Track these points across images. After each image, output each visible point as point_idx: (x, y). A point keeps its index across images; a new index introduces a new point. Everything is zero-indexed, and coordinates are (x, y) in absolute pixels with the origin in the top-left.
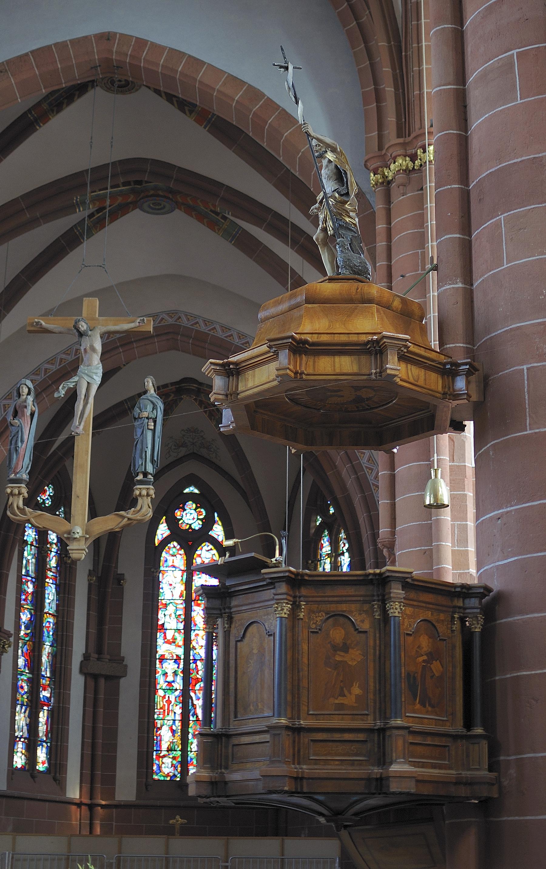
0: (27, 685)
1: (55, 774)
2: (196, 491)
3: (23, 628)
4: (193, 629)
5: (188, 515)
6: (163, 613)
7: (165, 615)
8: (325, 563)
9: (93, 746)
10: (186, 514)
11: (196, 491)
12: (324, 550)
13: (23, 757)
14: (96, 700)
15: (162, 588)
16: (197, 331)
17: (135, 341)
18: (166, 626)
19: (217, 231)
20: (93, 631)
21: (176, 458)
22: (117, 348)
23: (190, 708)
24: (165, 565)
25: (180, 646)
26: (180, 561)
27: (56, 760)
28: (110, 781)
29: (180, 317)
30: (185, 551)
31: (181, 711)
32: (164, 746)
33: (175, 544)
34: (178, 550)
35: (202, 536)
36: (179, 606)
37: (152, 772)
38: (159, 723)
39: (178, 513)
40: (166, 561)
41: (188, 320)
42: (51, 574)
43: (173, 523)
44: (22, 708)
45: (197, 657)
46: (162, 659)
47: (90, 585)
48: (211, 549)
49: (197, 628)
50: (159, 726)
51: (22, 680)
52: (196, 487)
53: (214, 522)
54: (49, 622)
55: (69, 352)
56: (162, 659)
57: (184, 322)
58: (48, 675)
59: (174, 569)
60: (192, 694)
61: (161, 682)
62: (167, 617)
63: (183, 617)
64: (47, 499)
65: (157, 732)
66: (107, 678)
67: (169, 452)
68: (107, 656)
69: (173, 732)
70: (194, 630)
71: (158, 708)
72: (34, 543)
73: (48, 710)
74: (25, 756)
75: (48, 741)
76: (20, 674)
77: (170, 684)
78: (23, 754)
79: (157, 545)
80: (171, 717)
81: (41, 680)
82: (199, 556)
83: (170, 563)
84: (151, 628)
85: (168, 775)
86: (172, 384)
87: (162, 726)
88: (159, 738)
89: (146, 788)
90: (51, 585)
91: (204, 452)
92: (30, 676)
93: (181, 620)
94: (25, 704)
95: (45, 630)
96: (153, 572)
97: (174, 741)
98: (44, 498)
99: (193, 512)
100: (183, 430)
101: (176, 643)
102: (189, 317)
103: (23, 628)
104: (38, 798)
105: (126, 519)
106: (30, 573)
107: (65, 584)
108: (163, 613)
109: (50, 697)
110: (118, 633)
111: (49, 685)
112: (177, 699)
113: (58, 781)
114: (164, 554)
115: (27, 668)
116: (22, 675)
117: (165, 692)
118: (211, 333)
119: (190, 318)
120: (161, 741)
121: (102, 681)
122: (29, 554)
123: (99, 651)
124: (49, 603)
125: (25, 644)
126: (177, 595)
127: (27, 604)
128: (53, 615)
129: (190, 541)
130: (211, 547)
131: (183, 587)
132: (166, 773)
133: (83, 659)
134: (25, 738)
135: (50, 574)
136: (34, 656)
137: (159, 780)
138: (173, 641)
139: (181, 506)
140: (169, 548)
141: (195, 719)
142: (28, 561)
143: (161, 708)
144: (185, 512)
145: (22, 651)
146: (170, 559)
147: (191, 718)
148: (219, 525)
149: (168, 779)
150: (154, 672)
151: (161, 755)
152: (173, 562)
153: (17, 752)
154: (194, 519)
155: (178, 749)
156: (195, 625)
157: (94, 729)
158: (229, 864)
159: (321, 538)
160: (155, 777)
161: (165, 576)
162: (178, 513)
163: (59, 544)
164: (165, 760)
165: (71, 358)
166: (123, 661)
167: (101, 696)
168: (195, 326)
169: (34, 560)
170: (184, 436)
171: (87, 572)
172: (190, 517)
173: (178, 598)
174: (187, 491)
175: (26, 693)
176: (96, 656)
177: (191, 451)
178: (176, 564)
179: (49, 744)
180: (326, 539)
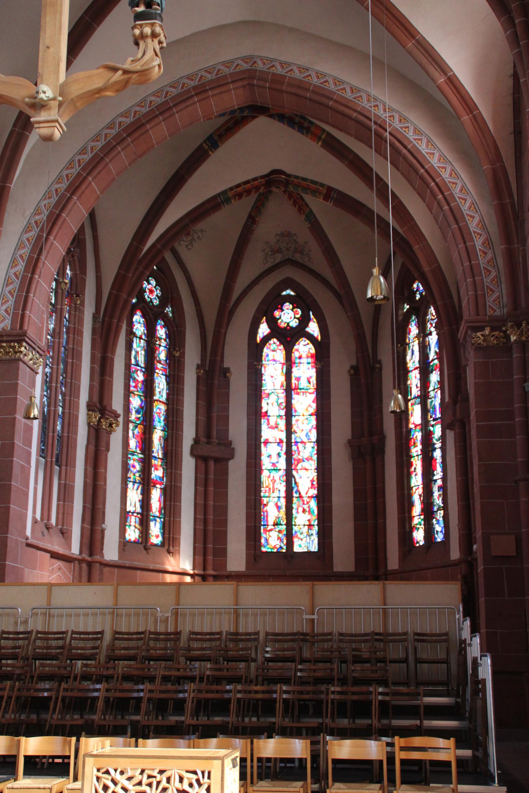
0: (139, 465)
1: (169, 546)
2: (292, 293)
3: (134, 412)
4: (294, 414)
5: (286, 314)
6: (266, 401)
7: (268, 404)
8: (413, 346)
9: (205, 521)
10: (284, 314)
11: (292, 293)
12: (412, 334)
13: (137, 531)
14: (206, 480)
15: (265, 380)
16: (273, 74)
18: (269, 414)
20: (202, 418)
21: (273, 264)
23: (293, 485)
24: (266, 360)
25: (282, 431)
26: (280, 355)
27: (169, 534)
28: (221, 553)
29: (255, 62)
30: (284, 346)
31: (285, 489)
32: (271, 521)
33: (275, 340)
34: (278, 346)
35: (300, 332)
36: (279, 395)
37: (260, 545)
38: (265, 500)
39: (277, 314)
40: (267, 356)
41: (264, 64)
42: (161, 366)
43: (273, 323)
44: (134, 485)
45: (299, 440)
46: (266, 442)
47: (198, 378)
48: (308, 344)
49: (297, 414)
50: (265, 502)
51: (134, 460)
52: (292, 290)
53: (309, 320)
54: (160, 409)
55: (143, 104)
56: (266, 442)
57: (260, 66)
58: (160, 456)
59: (275, 362)
60: (294, 473)
61: (266, 463)
62: (270, 405)
63: (284, 405)
64: (155, 299)
65: (264, 508)
66: (217, 460)
67: (266, 258)
68: (215, 440)
69: (278, 507)
70: (295, 416)
71: (264, 486)
72: (143, 337)
73: (161, 489)
74: (139, 529)
75: (161, 516)
76: (131, 454)
77: (274, 464)
78: (136, 527)
79: (258, 341)
80: (276, 494)
81: (153, 461)
82: (297, 350)
83: (271, 357)
84: (256, 415)
85: (275, 547)
86: (262, 177)
87: (268, 503)
88: (266, 513)
89: (255, 559)
90: (162, 376)
91: (298, 257)
92: (141, 456)
93: (282, 407)
94: (137, 482)
95: (156, 415)
96: (256, 365)
97: (280, 516)
98: (152, 297)
99: (290, 311)
100: (277, 234)
101: (279, 428)
103: (134, 412)
104: (151, 568)
105: (120, 72)
106: (140, 363)
107: (174, 375)
108: (266, 401)
109: (163, 477)
110: (226, 419)
111: (161, 466)
112: (281, 478)
113: (171, 554)
114: (265, 350)
115: (138, 449)
116: (133, 455)
117: (270, 472)
118: (289, 74)
120: (267, 516)
121: (212, 464)
122: (139, 347)
123: (209, 436)
124: (160, 392)
125: (136, 427)
126: (278, 386)
127: (137, 391)
128: (163, 403)
129: (288, 338)
130: (308, 341)
131: (283, 378)
132: (273, 546)
133: (193, 443)
134: (138, 513)
135: (159, 366)
136: (145, 438)
137: (267, 552)
138: (276, 426)
139: (280, 306)
140: (270, 344)
141: (298, 495)
142: (137, 352)
143: (267, 487)
144: (283, 312)
145: (133, 433)
146: (271, 355)
147: (295, 495)
148: (314, 322)
149: (275, 550)
150: (260, 454)
151: (268, 529)
152: (274, 357)
153: (130, 526)
154: (291, 318)
155: (283, 524)
156: (296, 411)
157: (205, 506)
158: (315, 617)
159: (408, 323)
160: (264, 549)
161: (266, 369)
162: (277, 314)
163: (168, 340)
164: (271, 533)
165: (146, 109)
166: (231, 444)
168: (271, 69)
169: (143, 352)
170: (279, 240)
171: (196, 366)
172: (288, 316)
173: (280, 388)
174: (284, 293)
175: (138, 471)
176: (205, 440)
177: (286, 257)
178: (276, 358)
179: (162, 520)
180: (413, 324)
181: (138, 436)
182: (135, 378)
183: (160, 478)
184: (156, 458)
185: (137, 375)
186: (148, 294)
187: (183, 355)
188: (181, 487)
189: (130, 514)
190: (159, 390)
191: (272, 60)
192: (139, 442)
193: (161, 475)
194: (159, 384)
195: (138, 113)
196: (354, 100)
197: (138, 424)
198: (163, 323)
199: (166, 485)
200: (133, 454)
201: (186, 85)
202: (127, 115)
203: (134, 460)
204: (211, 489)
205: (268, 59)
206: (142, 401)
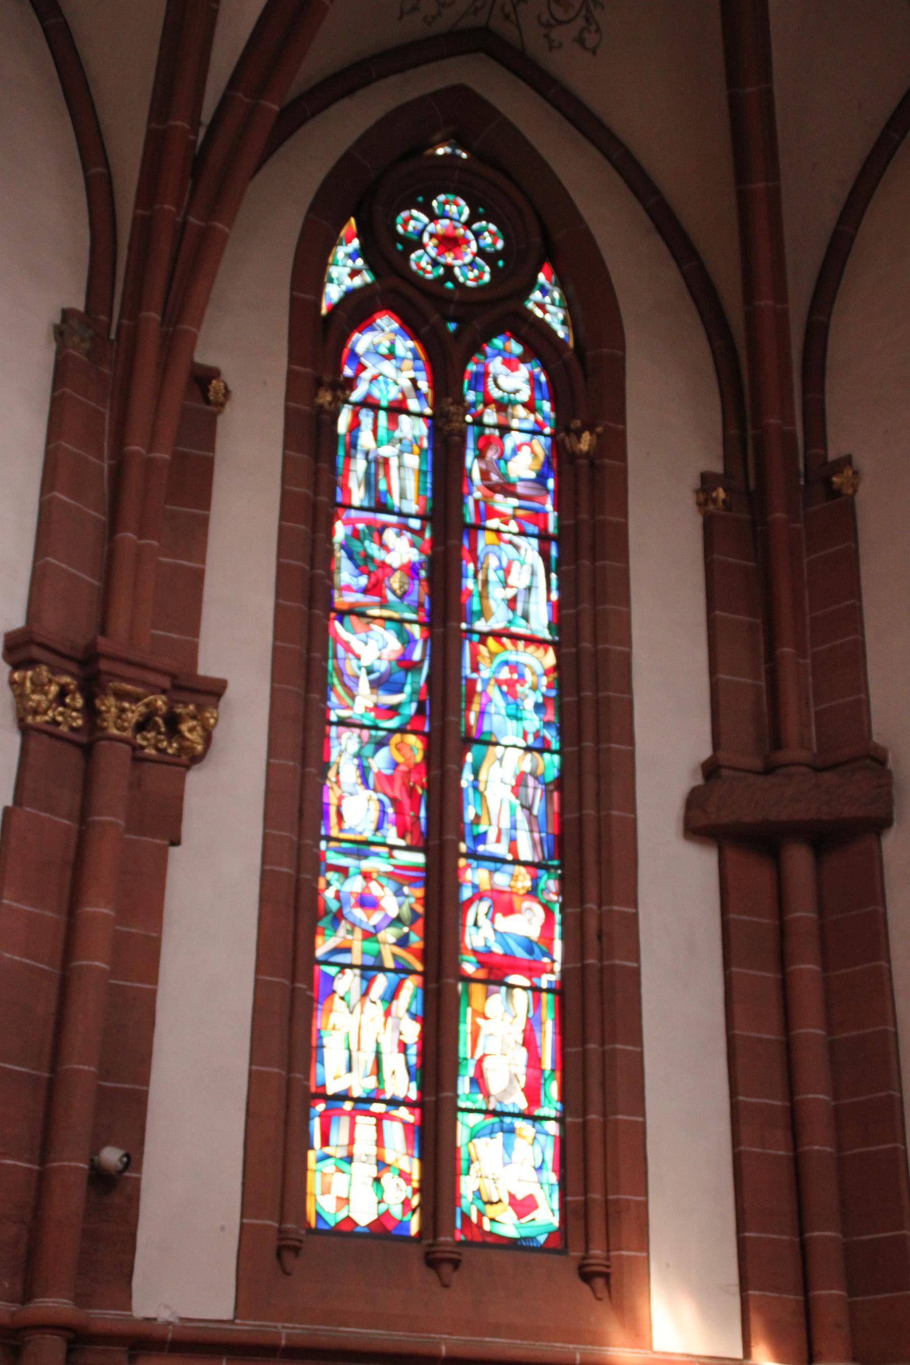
44: (371, 981)
51: (367, 876)
54: (514, 667)
58: (526, 853)
72: (413, 405)
90: (518, 540)
106: (395, 501)
113: (599, 1283)
116: (361, 855)
124: (512, 603)
125: (380, 744)
127: (384, 604)
134: (394, 1103)
145: (363, 772)
163: (546, 406)
167: (803, 913)
171: (694, 481)
175: (398, 920)
181: (390, 779)
182: (368, 558)
183: (529, 946)
184: (504, 861)
185: (383, 546)
186: (433, 252)
187: (614, 444)
188: (635, 975)
189: (348, 1106)
190: (510, 593)
192: (395, 801)
193: (534, 932)
194: (507, 572)
197: (392, 731)
198: (516, 348)
199: (563, 972)
200: (361, 848)
203: (367, 876)
204: (807, 967)
206: (408, 641)
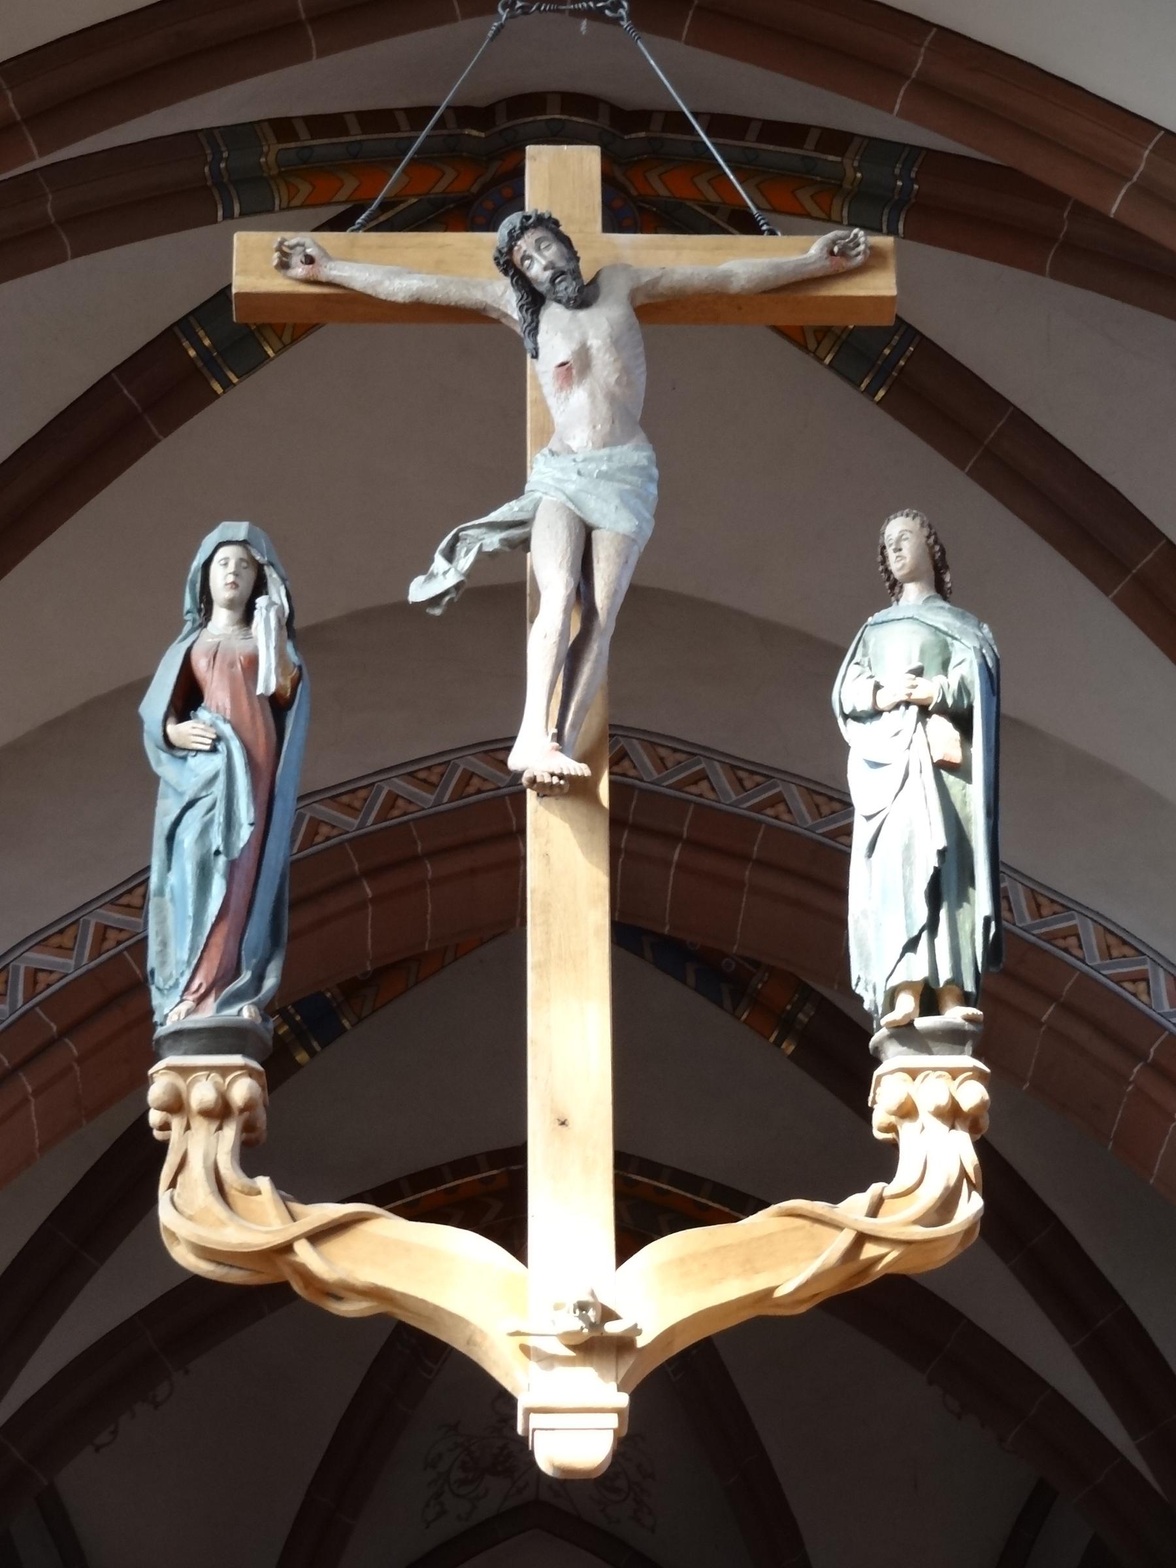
17: (431, 854)
19: (812, 345)
22: (351, 881)
41: (662, 763)
102: (663, 752)
118: (767, 817)
119: (671, 759)
168: (693, 789)
191: (694, 752)
195: (112, 936)
196: (1047, 946)
201: (324, 830)
202: (66, 940)
205: (679, 746)
